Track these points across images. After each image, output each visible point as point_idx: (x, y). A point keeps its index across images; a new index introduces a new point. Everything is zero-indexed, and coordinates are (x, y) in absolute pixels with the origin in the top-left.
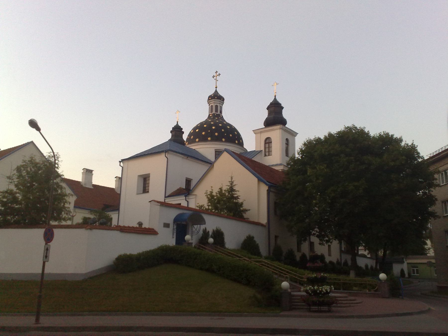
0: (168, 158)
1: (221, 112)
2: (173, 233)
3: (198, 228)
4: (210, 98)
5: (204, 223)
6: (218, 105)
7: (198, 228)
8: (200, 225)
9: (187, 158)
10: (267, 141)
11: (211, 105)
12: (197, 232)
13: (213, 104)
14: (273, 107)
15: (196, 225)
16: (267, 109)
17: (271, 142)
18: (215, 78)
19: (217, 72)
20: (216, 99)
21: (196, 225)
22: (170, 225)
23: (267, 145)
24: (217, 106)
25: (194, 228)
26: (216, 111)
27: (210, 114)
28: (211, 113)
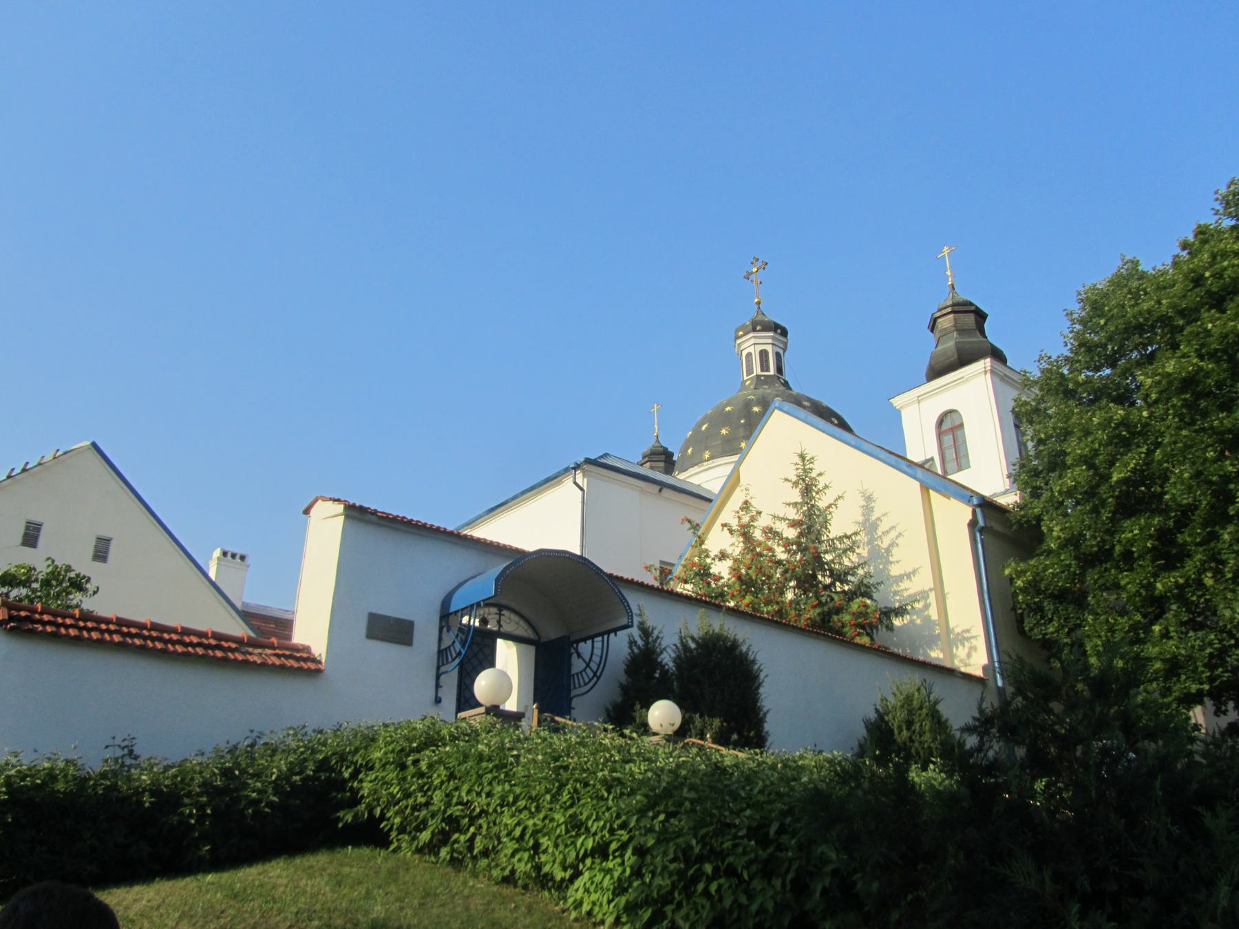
0: (585, 489)
1: (779, 370)
2: (438, 677)
3: (597, 652)
4: (741, 333)
5: (624, 621)
6: (769, 348)
7: (597, 652)
8: (606, 637)
9: (660, 491)
10: (947, 425)
11: (744, 353)
12: (595, 674)
13: (751, 350)
14: (951, 316)
15: (585, 640)
16: (932, 331)
17: (961, 426)
18: (751, 277)
19: (758, 260)
20: (759, 331)
21: (589, 642)
22: (417, 636)
23: (948, 439)
24: (764, 354)
25: (579, 656)
26: (765, 366)
27: (745, 378)
28: (747, 376)
